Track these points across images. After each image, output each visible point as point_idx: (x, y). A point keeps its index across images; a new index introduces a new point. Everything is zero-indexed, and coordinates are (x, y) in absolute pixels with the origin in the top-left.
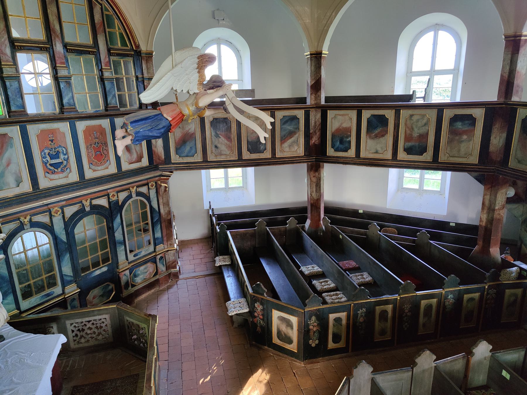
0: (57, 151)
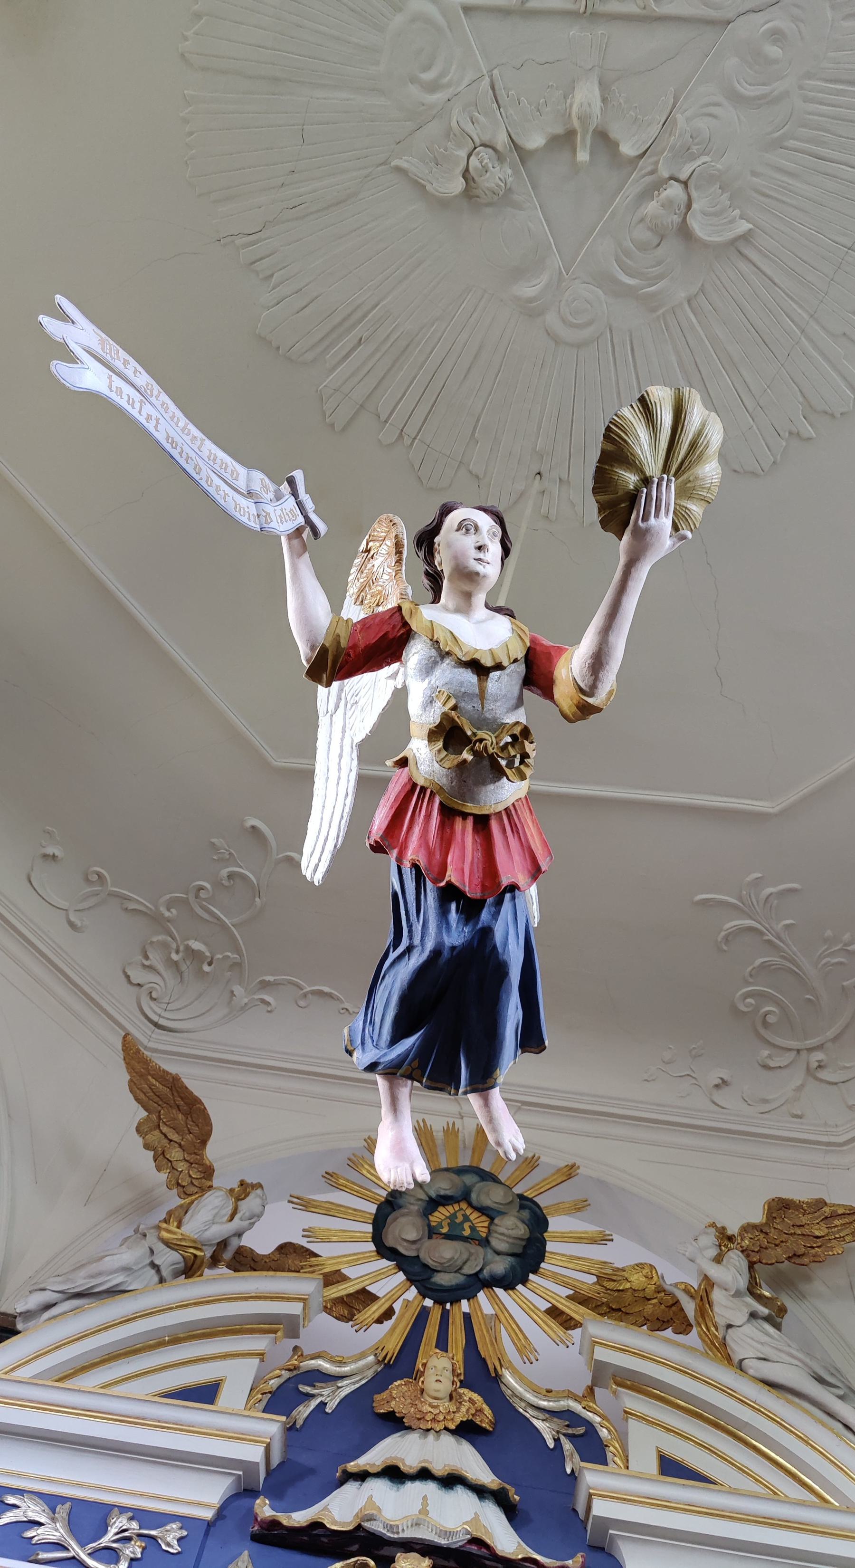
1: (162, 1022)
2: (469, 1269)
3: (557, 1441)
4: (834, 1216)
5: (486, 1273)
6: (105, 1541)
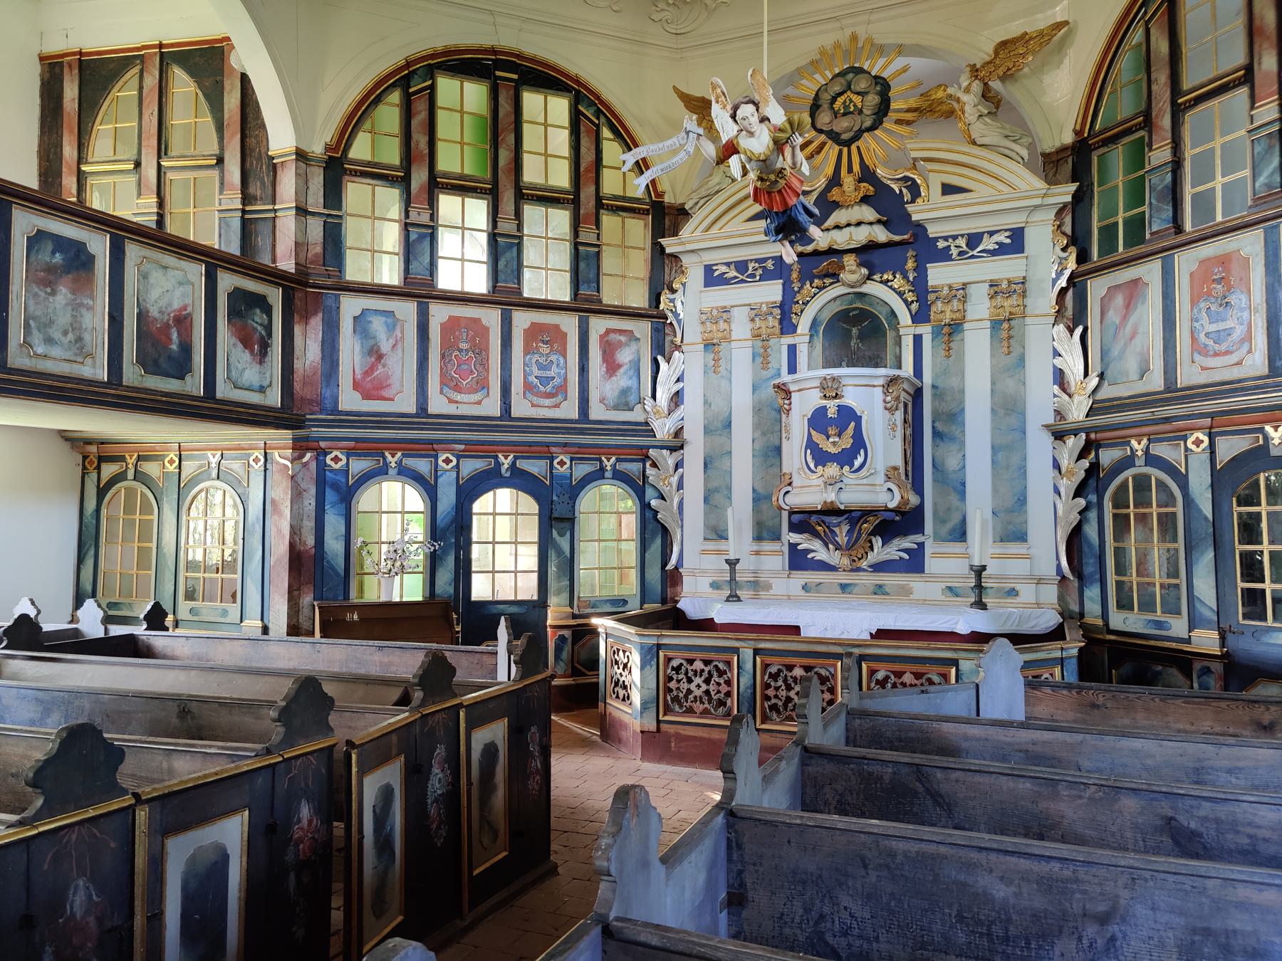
0: (1227, 303)
1: (679, 32)
2: (856, 128)
3: (901, 191)
4: (1031, 39)
5: (863, 127)
6: (749, 272)
